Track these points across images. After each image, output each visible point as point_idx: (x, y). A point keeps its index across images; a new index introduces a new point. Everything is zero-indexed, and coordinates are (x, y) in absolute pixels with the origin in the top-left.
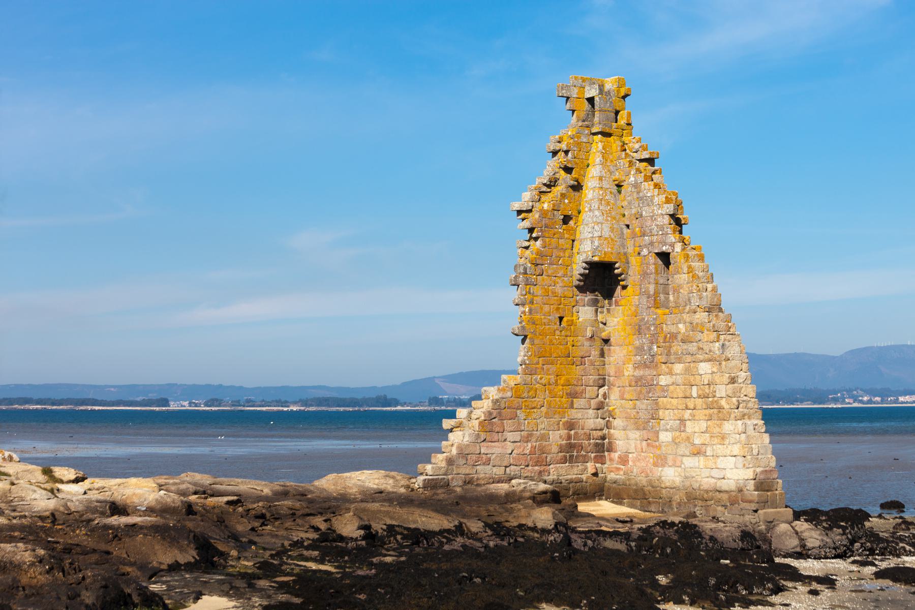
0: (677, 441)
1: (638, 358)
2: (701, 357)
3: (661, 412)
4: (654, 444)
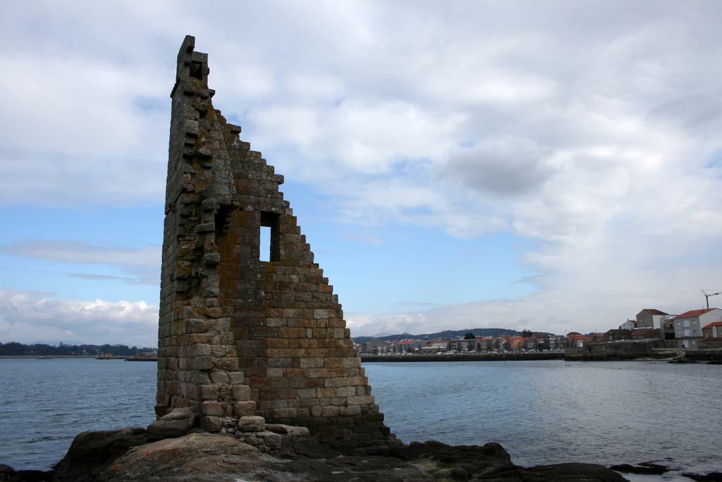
0: (290, 375)
1: (241, 301)
2: (317, 305)
3: (269, 351)
4: (261, 379)
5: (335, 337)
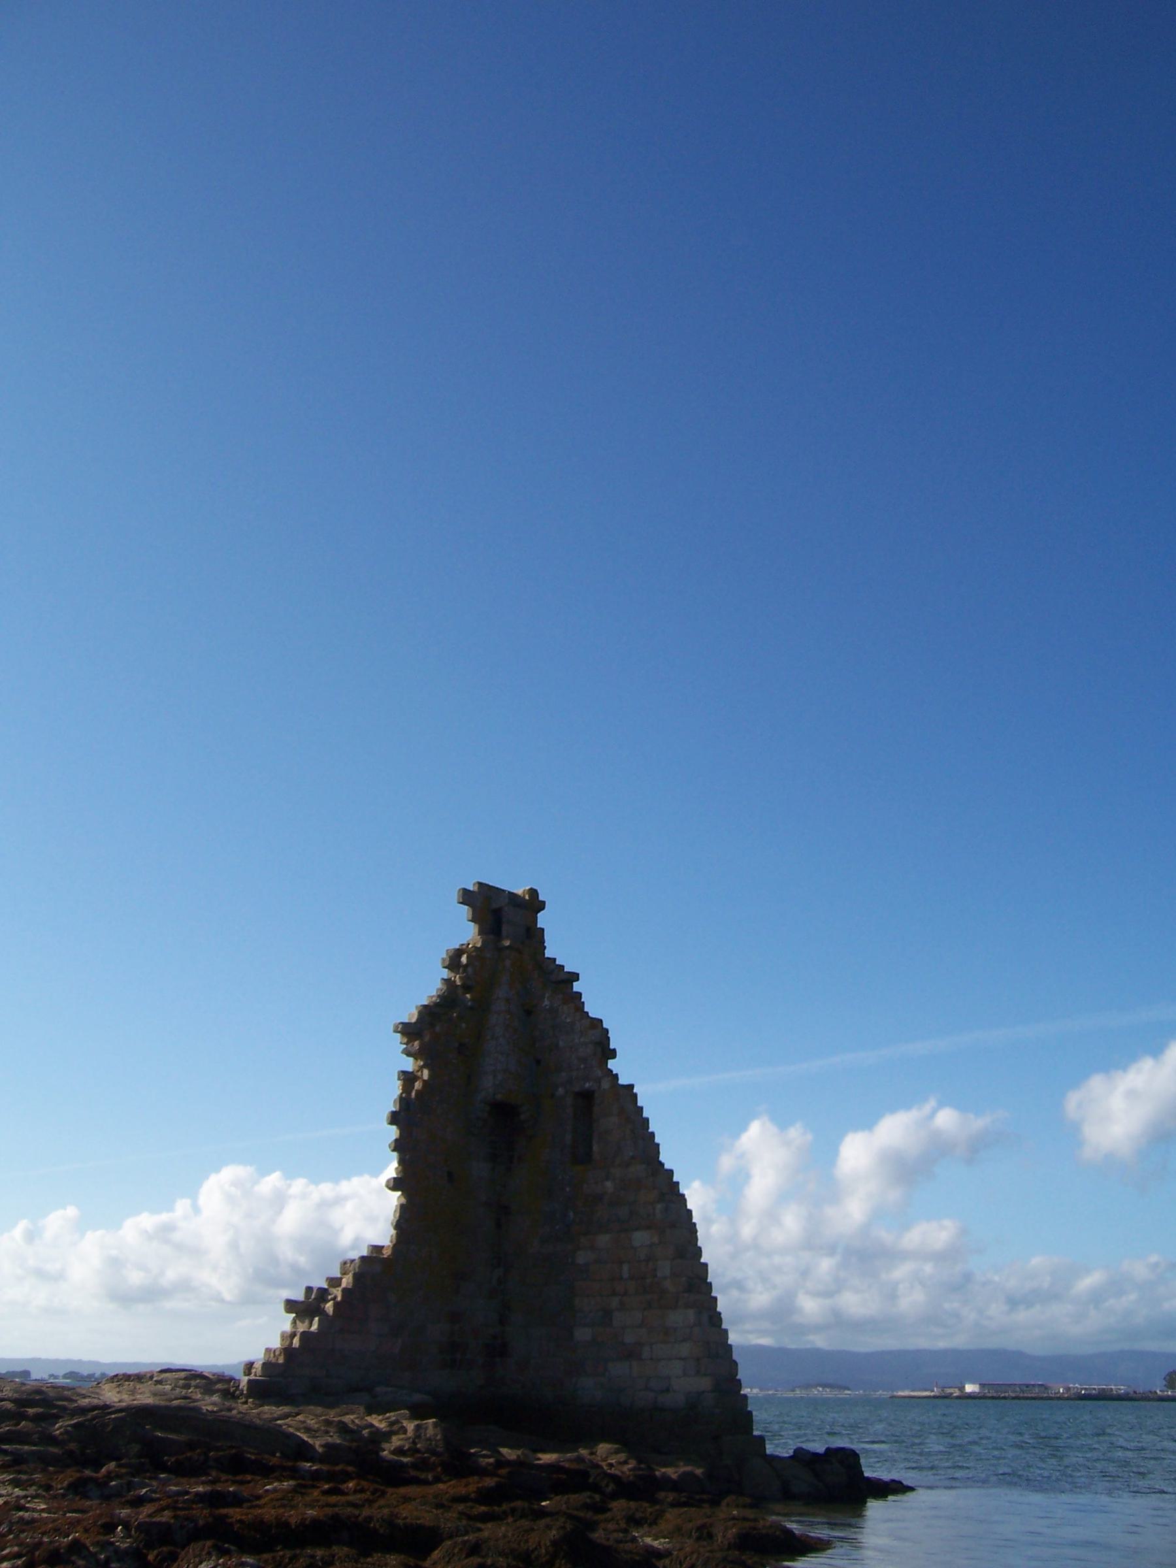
5: (659, 1274)
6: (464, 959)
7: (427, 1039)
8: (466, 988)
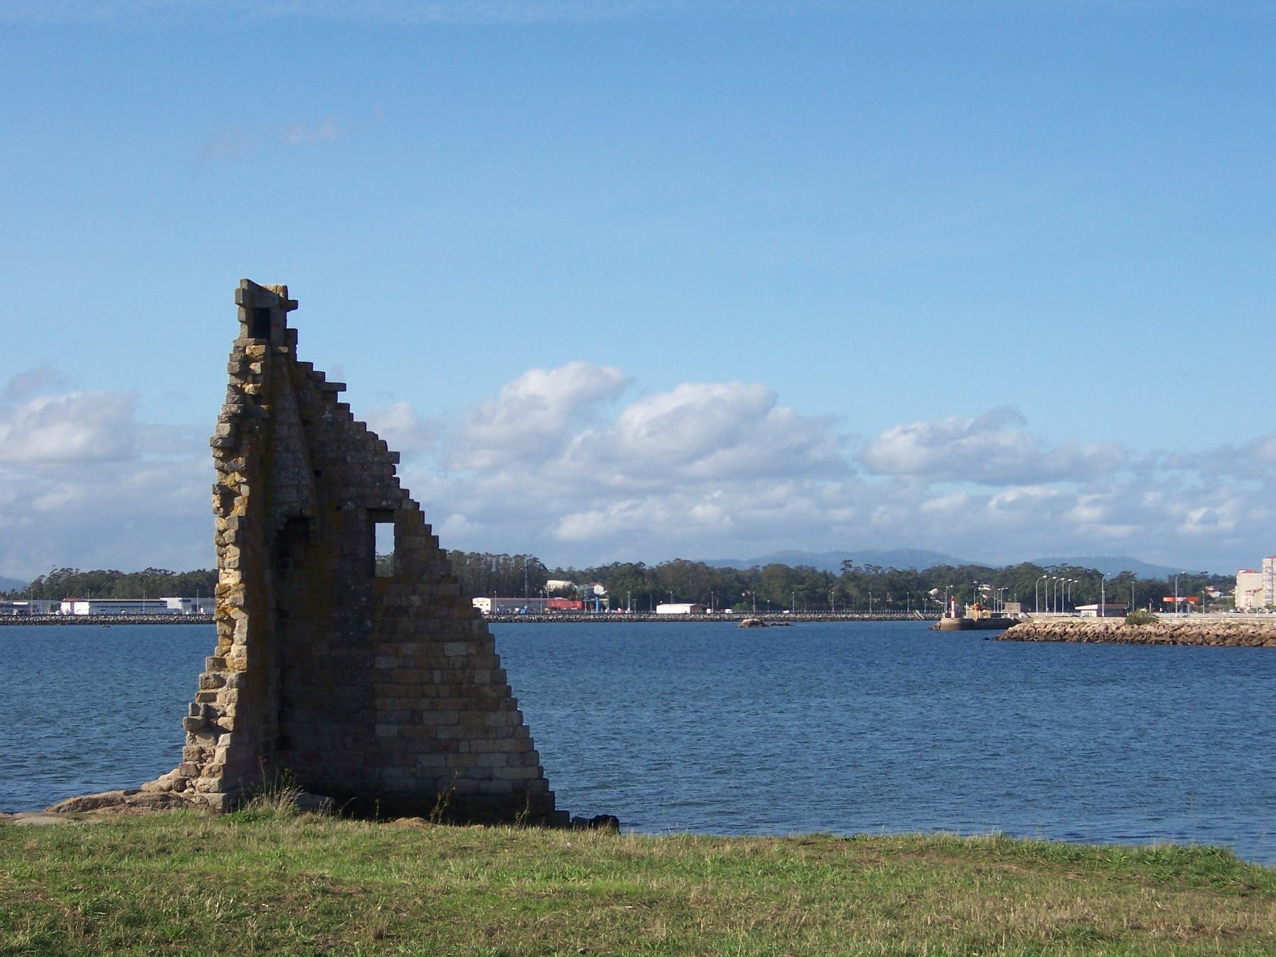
6: (256, 367)
7: (247, 454)
8: (257, 398)
